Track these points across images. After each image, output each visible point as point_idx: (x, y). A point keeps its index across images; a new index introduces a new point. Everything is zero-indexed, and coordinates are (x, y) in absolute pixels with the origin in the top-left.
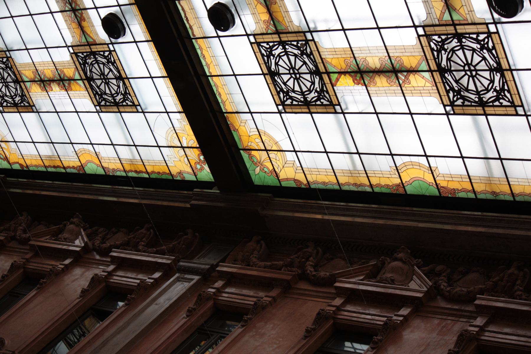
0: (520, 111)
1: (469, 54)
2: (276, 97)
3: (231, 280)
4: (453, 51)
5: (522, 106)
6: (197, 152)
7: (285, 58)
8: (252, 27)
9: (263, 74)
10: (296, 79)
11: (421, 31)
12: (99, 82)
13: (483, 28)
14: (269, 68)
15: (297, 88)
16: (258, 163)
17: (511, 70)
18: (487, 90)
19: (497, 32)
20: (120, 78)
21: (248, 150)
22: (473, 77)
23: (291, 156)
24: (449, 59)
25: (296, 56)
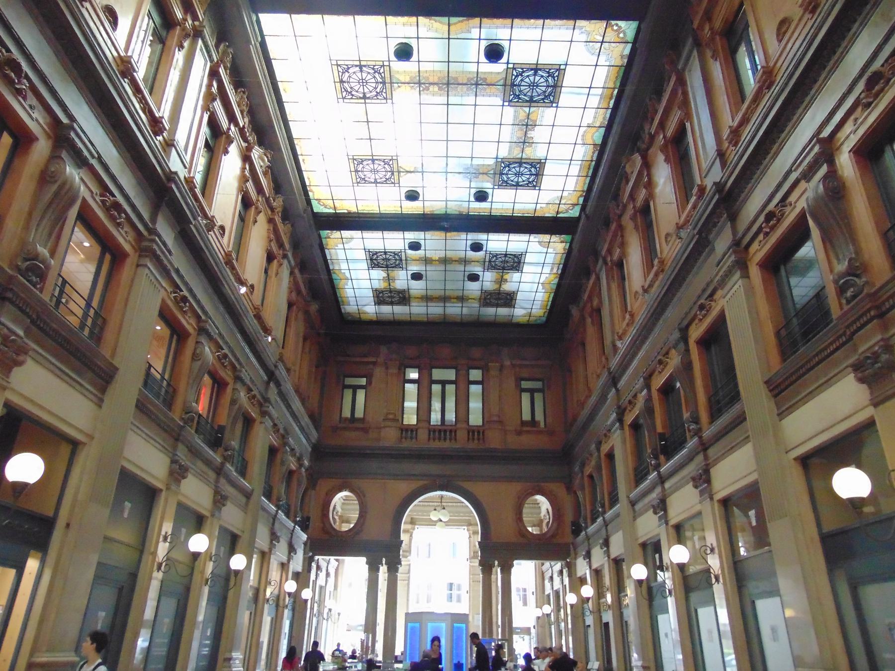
0: (562, 67)
1: (523, 83)
3: (610, 251)
4: (520, 91)
6: (553, 236)
8: (489, 185)
11: (506, 104)
13: (510, 71)
16: (567, 211)
17: (537, 64)
18: (547, 81)
20: (506, 255)
21: (558, 213)
22: (537, 86)
23: (565, 194)
24: (525, 95)
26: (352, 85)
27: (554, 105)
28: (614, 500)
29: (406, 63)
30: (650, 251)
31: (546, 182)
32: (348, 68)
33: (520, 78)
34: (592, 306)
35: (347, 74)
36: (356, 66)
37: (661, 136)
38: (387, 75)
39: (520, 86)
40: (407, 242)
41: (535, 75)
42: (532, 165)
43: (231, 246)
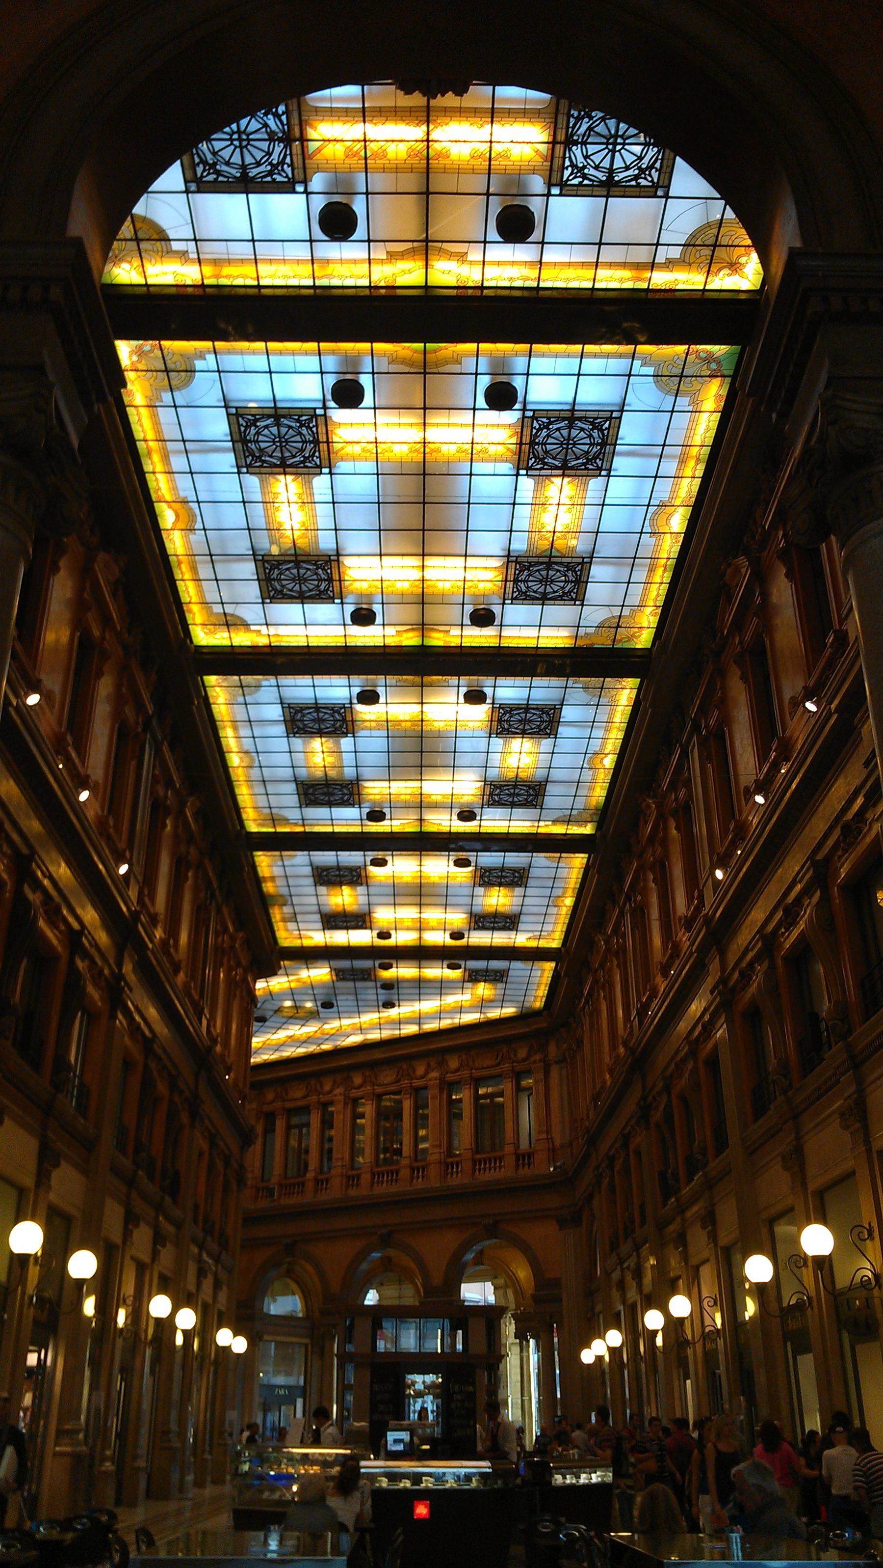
0: (615, 415)
1: (550, 440)
2: (566, 602)
3: (703, 711)
5: (612, 411)
7: (530, 584)
9: (543, 604)
10: (552, 581)
12: (527, 727)
14: (537, 599)
15: (562, 584)
17: (573, 410)
18: (590, 436)
19: (534, 411)
22: (574, 444)
24: (554, 458)
25: (529, 575)
26: (263, 445)
27: (603, 473)
28: (721, 1143)
29: (354, 410)
30: (767, 730)
31: (593, 591)
32: (257, 420)
33: (544, 433)
34: (676, 799)
35: (253, 431)
36: (269, 416)
37: (781, 533)
38: (321, 429)
39: (545, 444)
40: (356, 691)
41: (570, 427)
42: (569, 567)
43: (65, 723)
